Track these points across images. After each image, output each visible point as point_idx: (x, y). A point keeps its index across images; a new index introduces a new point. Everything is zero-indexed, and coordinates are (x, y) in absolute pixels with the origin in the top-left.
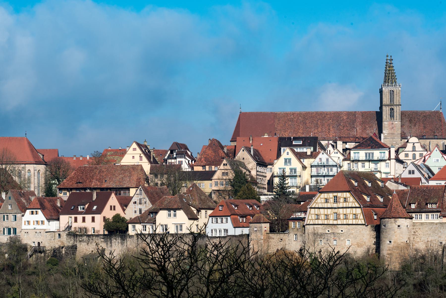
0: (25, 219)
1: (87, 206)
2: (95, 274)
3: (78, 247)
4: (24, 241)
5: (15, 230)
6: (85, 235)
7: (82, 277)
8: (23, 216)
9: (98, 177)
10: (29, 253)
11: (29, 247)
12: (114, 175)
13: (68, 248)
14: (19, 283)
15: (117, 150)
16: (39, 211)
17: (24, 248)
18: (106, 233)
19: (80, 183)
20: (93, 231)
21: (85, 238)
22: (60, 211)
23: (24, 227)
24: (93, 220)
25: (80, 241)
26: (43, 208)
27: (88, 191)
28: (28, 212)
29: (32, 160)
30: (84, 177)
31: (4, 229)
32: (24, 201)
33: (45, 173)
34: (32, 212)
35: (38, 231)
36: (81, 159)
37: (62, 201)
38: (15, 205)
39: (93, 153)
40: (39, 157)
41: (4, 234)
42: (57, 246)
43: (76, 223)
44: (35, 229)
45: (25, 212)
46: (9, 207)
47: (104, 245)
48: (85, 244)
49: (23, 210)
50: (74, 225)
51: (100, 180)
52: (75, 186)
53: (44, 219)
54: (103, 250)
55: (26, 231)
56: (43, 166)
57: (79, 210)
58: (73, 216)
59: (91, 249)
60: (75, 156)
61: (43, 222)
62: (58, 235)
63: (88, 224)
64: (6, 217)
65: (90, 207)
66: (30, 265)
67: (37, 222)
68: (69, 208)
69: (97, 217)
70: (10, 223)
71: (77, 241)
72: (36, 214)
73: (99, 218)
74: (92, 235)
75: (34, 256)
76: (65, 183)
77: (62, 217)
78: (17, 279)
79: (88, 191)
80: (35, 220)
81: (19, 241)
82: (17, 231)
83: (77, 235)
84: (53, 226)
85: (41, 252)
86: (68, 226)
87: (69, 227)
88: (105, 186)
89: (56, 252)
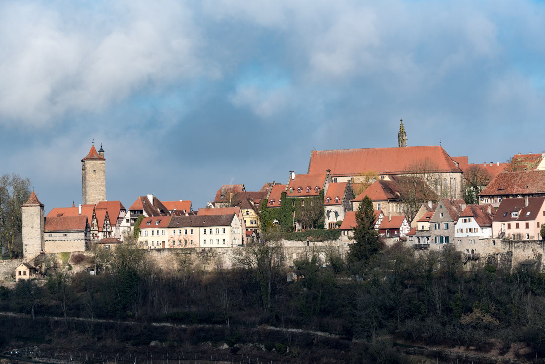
0: (457, 227)
1: (520, 212)
2: (538, 279)
3: (513, 253)
4: (458, 250)
5: (447, 238)
6: (521, 241)
7: (525, 283)
8: (455, 224)
9: (519, 184)
10: (463, 261)
11: (462, 254)
12: (536, 180)
13: (503, 254)
14: (461, 290)
15: (527, 155)
16: (472, 219)
17: (458, 256)
18: (541, 238)
19: (501, 189)
20: (527, 237)
21: (520, 244)
22: (492, 218)
23: (456, 235)
24: (527, 226)
25: (516, 248)
26: (475, 216)
27: (520, 197)
28: (461, 220)
29: (447, 168)
30: (505, 183)
31: (436, 237)
32: (455, 209)
33: (461, 181)
34: (465, 220)
35: (471, 239)
36: (491, 165)
37: (493, 209)
38: (447, 214)
39: (509, 159)
40: (454, 165)
41: (436, 242)
42: (492, 253)
43: (509, 230)
44: (468, 236)
45: (457, 220)
46: (441, 216)
47: (540, 251)
48: (521, 250)
49: (455, 218)
50: (508, 232)
51: (521, 186)
52: (497, 193)
53: (477, 226)
54: (540, 256)
55: (459, 239)
56: (459, 174)
57: (512, 216)
58: (506, 223)
59: (527, 256)
60: (485, 163)
61: (476, 230)
62: (492, 242)
63: (523, 230)
64: (437, 225)
65: (524, 213)
66: (466, 272)
67: (471, 230)
68: (503, 215)
69: (531, 223)
70: (442, 231)
71: (512, 248)
72: (469, 221)
73: (532, 223)
74: (528, 241)
75: (468, 264)
76: (486, 190)
77: (495, 224)
78: (459, 286)
79: (520, 197)
80: (468, 228)
81: (454, 249)
82: (450, 239)
83: (512, 241)
84: (486, 233)
85: (476, 260)
86: (501, 233)
87: (503, 234)
88: (527, 191)
89: (491, 259)
